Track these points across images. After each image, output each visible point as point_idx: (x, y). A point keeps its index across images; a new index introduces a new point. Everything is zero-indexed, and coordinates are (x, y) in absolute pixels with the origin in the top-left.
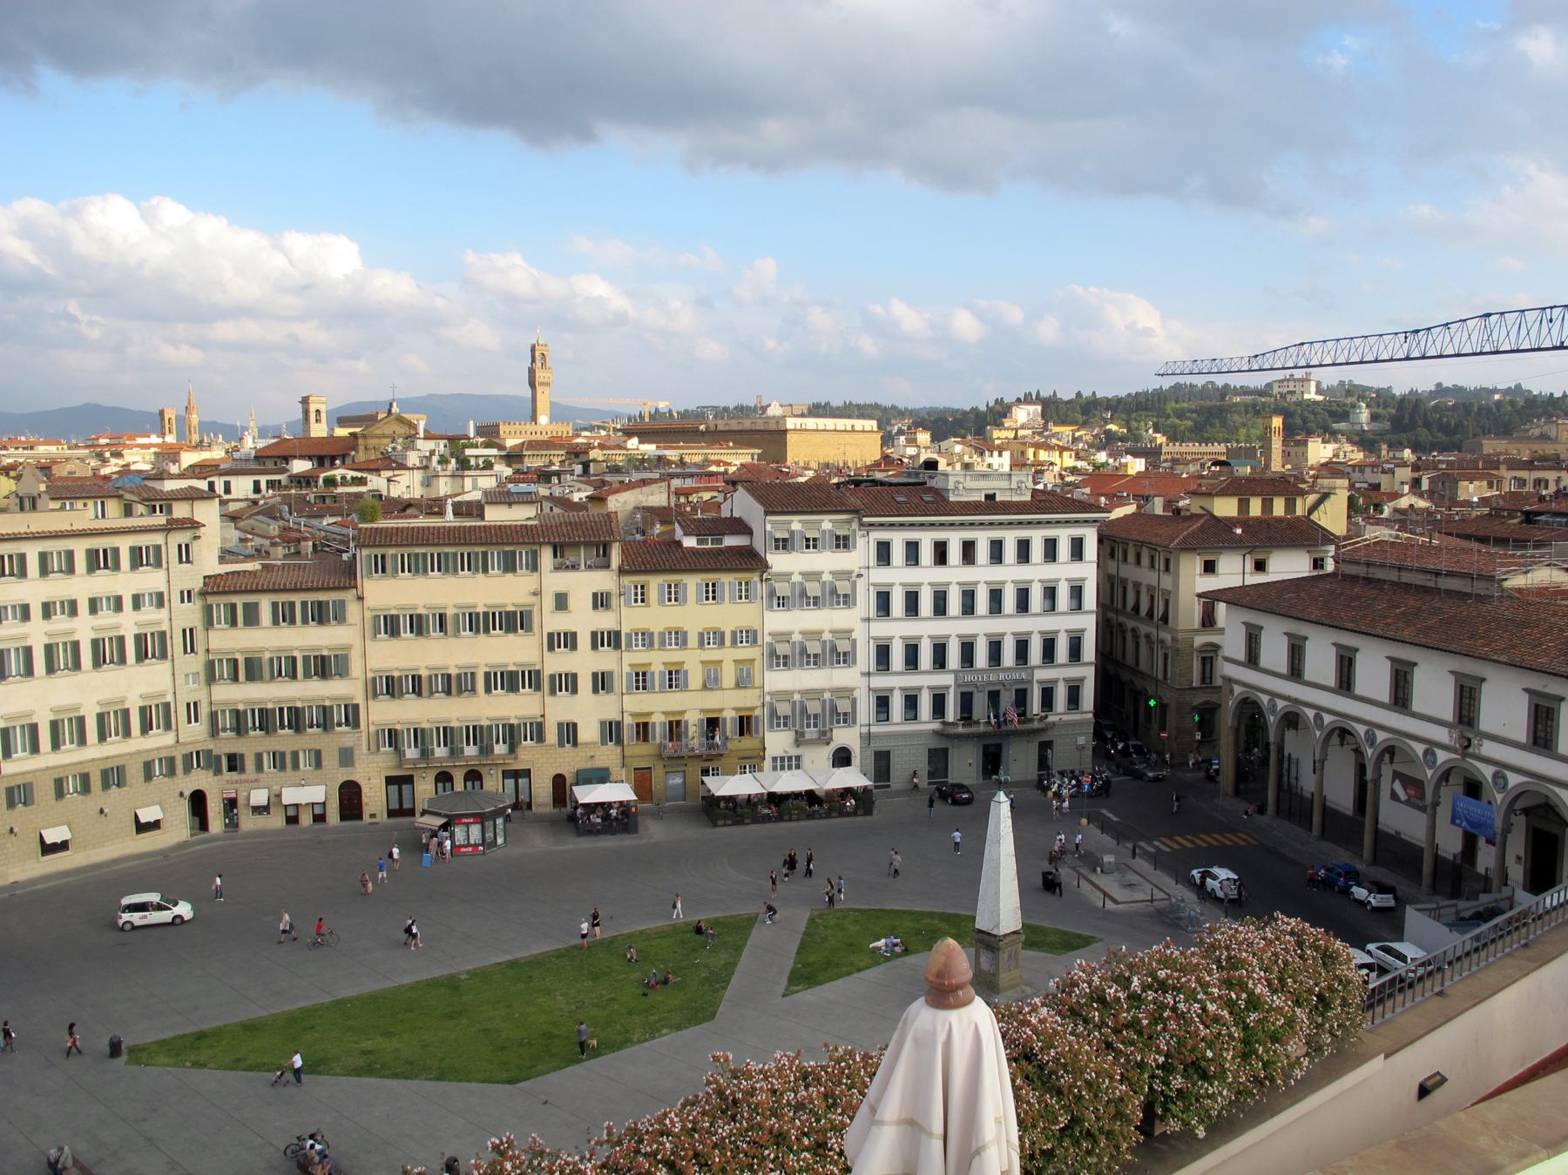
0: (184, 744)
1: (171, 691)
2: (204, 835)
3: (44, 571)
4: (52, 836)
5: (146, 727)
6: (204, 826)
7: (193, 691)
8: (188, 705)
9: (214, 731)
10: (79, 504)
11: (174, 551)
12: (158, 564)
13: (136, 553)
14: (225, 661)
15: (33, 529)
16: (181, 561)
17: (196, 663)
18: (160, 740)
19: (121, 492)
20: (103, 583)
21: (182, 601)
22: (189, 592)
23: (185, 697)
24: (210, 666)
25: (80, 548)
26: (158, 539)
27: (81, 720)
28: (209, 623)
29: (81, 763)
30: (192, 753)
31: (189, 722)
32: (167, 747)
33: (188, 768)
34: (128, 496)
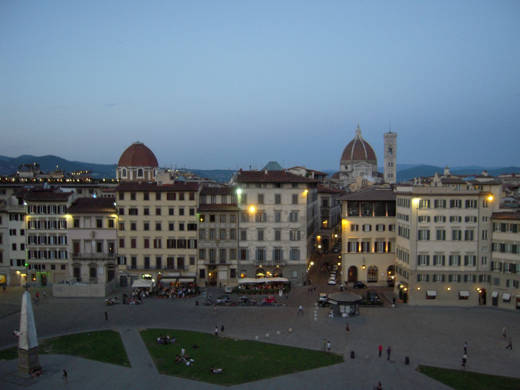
0: (480, 271)
1: (477, 251)
2: (484, 306)
3: (436, 206)
4: (431, 293)
5: (466, 263)
6: (485, 303)
7: (485, 253)
8: (483, 258)
9: (492, 268)
10: (451, 185)
11: (481, 203)
12: (475, 207)
13: (467, 202)
14: (498, 244)
15: (434, 192)
16: (484, 206)
17: (487, 243)
18: (471, 268)
19: (466, 182)
20: (455, 212)
21: (483, 221)
22: (486, 218)
23: (481, 255)
24: (493, 245)
25: (448, 199)
26: (476, 198)
27: (444, 257)
28: (494, 229)
29: (442, 271)
30: (482, 275)
31: (483, 264)
32: (473, 271)
33: (481, 280)
34: (468, 183)
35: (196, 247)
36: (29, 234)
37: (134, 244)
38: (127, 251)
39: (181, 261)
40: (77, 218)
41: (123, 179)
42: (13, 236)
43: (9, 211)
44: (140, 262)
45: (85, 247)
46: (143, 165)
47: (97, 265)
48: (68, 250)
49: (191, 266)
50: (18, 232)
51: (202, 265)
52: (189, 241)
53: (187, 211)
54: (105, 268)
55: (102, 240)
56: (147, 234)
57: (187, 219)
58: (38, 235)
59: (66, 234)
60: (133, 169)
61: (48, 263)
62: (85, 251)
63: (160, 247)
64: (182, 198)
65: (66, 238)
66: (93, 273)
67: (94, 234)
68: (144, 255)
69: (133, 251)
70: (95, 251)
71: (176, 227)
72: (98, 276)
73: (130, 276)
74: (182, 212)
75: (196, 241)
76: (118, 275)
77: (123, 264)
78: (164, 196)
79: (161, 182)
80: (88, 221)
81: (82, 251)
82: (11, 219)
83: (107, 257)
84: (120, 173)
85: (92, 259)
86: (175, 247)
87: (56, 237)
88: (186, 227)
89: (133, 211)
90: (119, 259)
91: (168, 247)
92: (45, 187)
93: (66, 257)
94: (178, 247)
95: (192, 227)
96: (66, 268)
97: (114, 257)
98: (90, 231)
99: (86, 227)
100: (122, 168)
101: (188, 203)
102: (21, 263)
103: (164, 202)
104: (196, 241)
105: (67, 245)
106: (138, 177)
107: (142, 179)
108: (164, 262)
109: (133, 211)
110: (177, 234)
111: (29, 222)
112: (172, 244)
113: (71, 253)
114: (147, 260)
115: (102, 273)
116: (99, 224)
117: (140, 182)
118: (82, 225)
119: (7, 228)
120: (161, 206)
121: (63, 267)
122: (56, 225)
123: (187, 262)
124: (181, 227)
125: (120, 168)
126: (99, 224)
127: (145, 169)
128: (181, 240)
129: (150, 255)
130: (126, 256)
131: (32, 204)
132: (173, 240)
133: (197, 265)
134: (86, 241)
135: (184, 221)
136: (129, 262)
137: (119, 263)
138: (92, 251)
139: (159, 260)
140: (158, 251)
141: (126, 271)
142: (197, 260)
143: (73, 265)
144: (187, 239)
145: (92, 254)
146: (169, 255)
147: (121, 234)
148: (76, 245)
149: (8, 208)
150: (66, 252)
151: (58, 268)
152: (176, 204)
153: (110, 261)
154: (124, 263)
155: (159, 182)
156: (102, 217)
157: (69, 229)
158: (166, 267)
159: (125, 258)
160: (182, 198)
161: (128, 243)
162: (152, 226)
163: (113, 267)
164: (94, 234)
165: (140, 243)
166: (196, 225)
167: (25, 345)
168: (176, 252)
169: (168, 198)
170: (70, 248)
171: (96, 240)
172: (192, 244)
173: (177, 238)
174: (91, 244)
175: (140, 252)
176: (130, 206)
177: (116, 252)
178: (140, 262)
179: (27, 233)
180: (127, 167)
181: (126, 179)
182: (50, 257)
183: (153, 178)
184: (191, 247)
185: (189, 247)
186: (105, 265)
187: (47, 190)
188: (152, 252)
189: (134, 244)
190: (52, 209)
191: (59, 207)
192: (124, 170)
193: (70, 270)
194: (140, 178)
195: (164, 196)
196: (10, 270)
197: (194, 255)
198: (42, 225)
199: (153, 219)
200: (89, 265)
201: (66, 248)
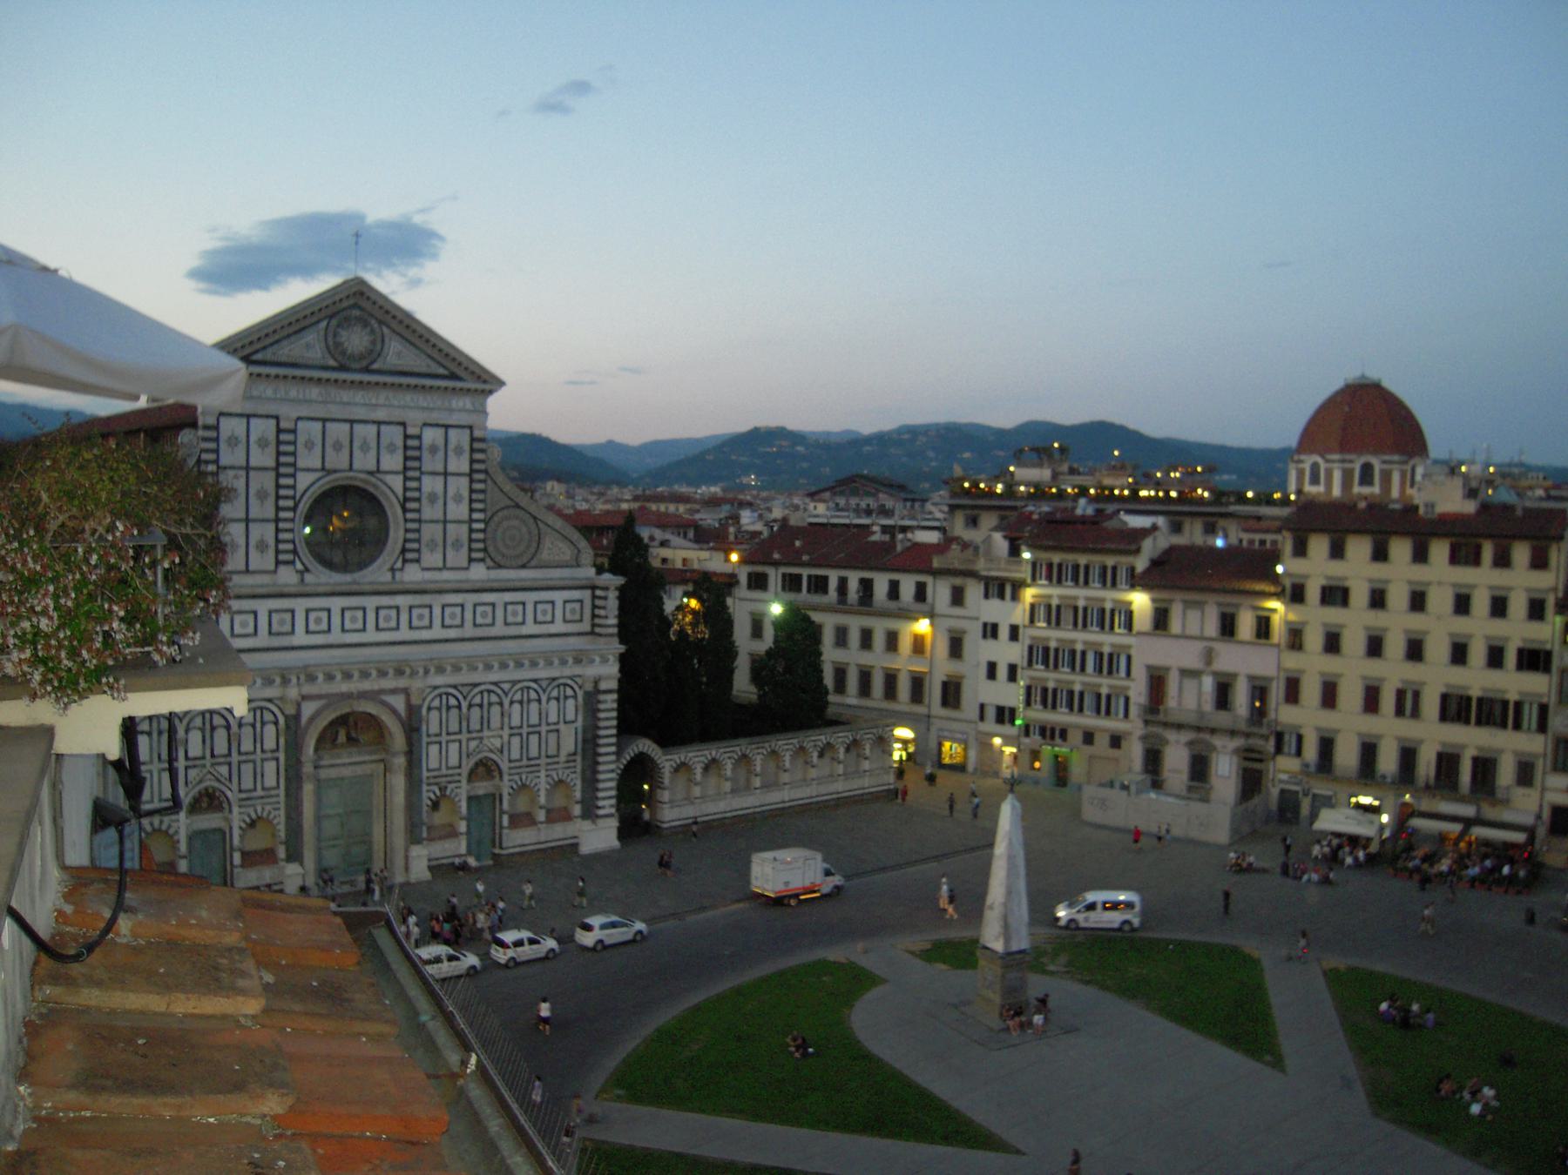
35: (1542, 727)
36: (1033, 638)
37: (1329, 696)
38: (1306, 717)
39: (1485, 767)
40: (1164, 605)
41: (1309, 493)
42: (990, 642)
43: (984, 573)
44: (1347, 756)
45: (1180, 689)
46: (1376, 451)
47: (1214, 748)
48: (1132, 694)
49: (1519, 793)
50: (1004, 632)
51: (1556, 790)
52: (1518, 706)
53: (1518, 606)
54: (1235, 759)
55: (1234, 676)
56: (1374, 668)
57: (1517, 631)
58: (1053, 645)
59: (1129, 647)
60: (1343, 461)
61: (1077, 727)
62: (1180, 703)
63: (1416, 713)
64: (1503, 561)
65: (1129, 658)
66: (1200, 769)
67: (1209, 656)
68: (1359, 734)
69: (1328, 719)
70: (1208, 705)
71: (1477, 654)
72: (1215, 781)
73: (1310, 797)
74: (1499, 607)
75: (1543, 710)
76: (1274, 786)
77: (1289, 754)
78: (1439, 551)
79: (1433, 506)
80: (1193, 615)
81: (1171, 702)
82: (986, 596)
83: (1242, 726)
84: (1301, 473)
85: (1199, 729)
86: (1467, 722)
87: (1101, 655)
88: (1511, 658)
89: (1335, 595)
90: (1279, 737)
91: (1444, 716)
92: (1079, 512)
93: (1126, 715)
94: (1479, 723)
95: (1533, 659)
96: (1124, 744)
97: (1264, 731)
98: (1199, 646)
99: (1188, 632)
100: (1308, 460)
101: (1521, 580)
102: (1004, 715)
103: (1440, 572)
104: (1543, 710)
105: (1133, 680)
106: (1357, 489)
107: (1372, 495)
108: (1426, 765)
109: (1335, 595)
110: (1476, 679)
111: (1033, 606)
112: (1456, 708)
113: (1139, 705)
114: (1369, 751)
115: (1227, 774)
116: (1228, 627)
117: (1362, 505)
118: (1175, 626)
119: (977, 619)
120: (1429, 584)
121: (1116, 741)
122: (1102, 619)
123: (1506, 774)
124: (1495, 657)
125: (1303, 457)
126: (1228, 627)
127: (1384, 462)
128: (1491, 701)
129: (1379, 737)
130: (1303, 731)
131: (1045, 556)
132: (1461, 697)
133: (1544, 789)
134: (1186, 673)
135: (1507, 639)
136: (1311, 752)
137: (1279, 749)
138: (1199, 705)
139: (1408, 756)
140: (1407, 729)
141: (1300, 777)
142: (1544, 773)
143: (1144, 738)
144: (1512, 697)
145: (1201, 714)
146: (1444, 744)
147: (1292, 661)
148: (1157, 682)
149: (981, 566)
150: (1127, 699)
151: (1102, 741)
152: (1482, 579)
153: (1257, 742)
154: (1293, 750)
155: (1426, 505)
156: (1237, 606)
157: (1139, 633)
158: (1432, 781)
159: (1300, 738)
160: (1503, 561)
161: (1311, 691)
162: (1395, 646)
163: (1261, 761)
164: (1209, 656)
165: (1349, 695)
166: (1548, 654)
167: (997, 939)
168: (1472, 739)
169: (1454, 559)
170: (1138, 691)
171: (1215, 674)
172: (1530, 716)
173: (1475, 693)
174: (1200, 684)
175: (1349, 723)
176: (1328, 578)
177: (1272, 715)
178: (1347, 756)
179: (1026, 635)
180: (1323, 457)
181: (1319, 494)
182: (1081, 710)
183: (1409, 491)
184: (1525, 724)
185: (1517, 726)
186: (1236, 751)
187: (1084, 520)
188: (1389, 729)
189: (1329, 696)
190: (1095, 573)
191: (1114, 569)
192: (1315, 467)
193: (1135, 752)
194: (1366, 490)
195: (1439, 551)
196: (979, 732)
197: (1536, 756)
198: (1067, 616)
199: (1397, 623)
200: (1190, 744)
201: (1127, 688)
